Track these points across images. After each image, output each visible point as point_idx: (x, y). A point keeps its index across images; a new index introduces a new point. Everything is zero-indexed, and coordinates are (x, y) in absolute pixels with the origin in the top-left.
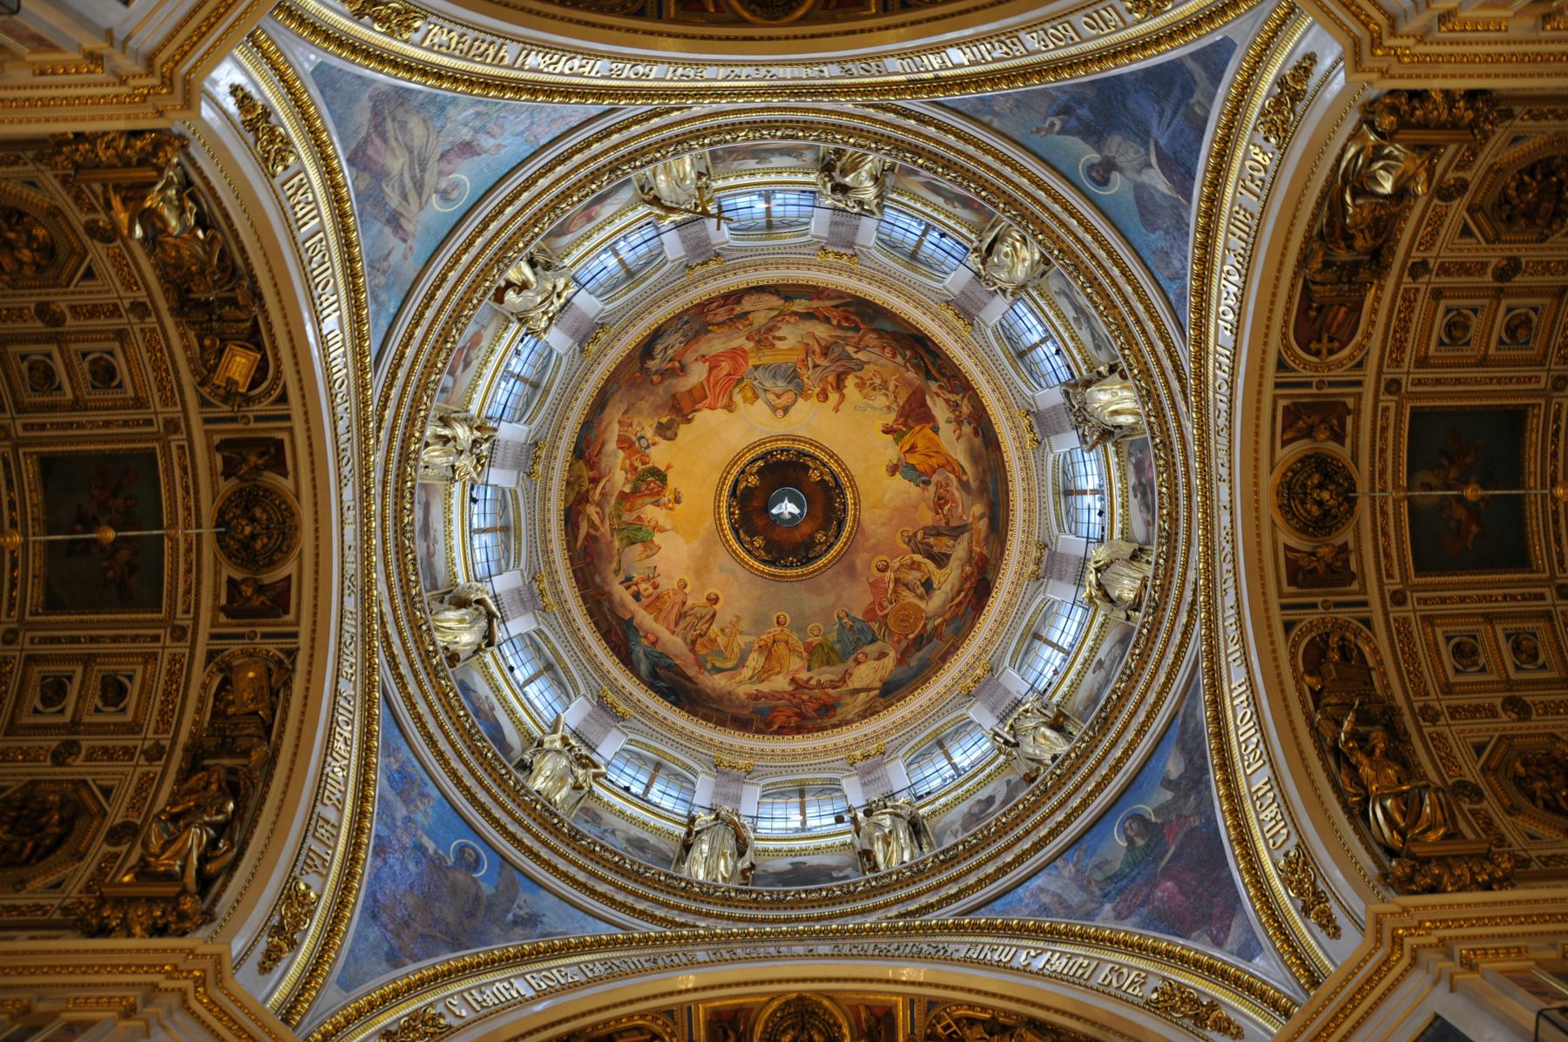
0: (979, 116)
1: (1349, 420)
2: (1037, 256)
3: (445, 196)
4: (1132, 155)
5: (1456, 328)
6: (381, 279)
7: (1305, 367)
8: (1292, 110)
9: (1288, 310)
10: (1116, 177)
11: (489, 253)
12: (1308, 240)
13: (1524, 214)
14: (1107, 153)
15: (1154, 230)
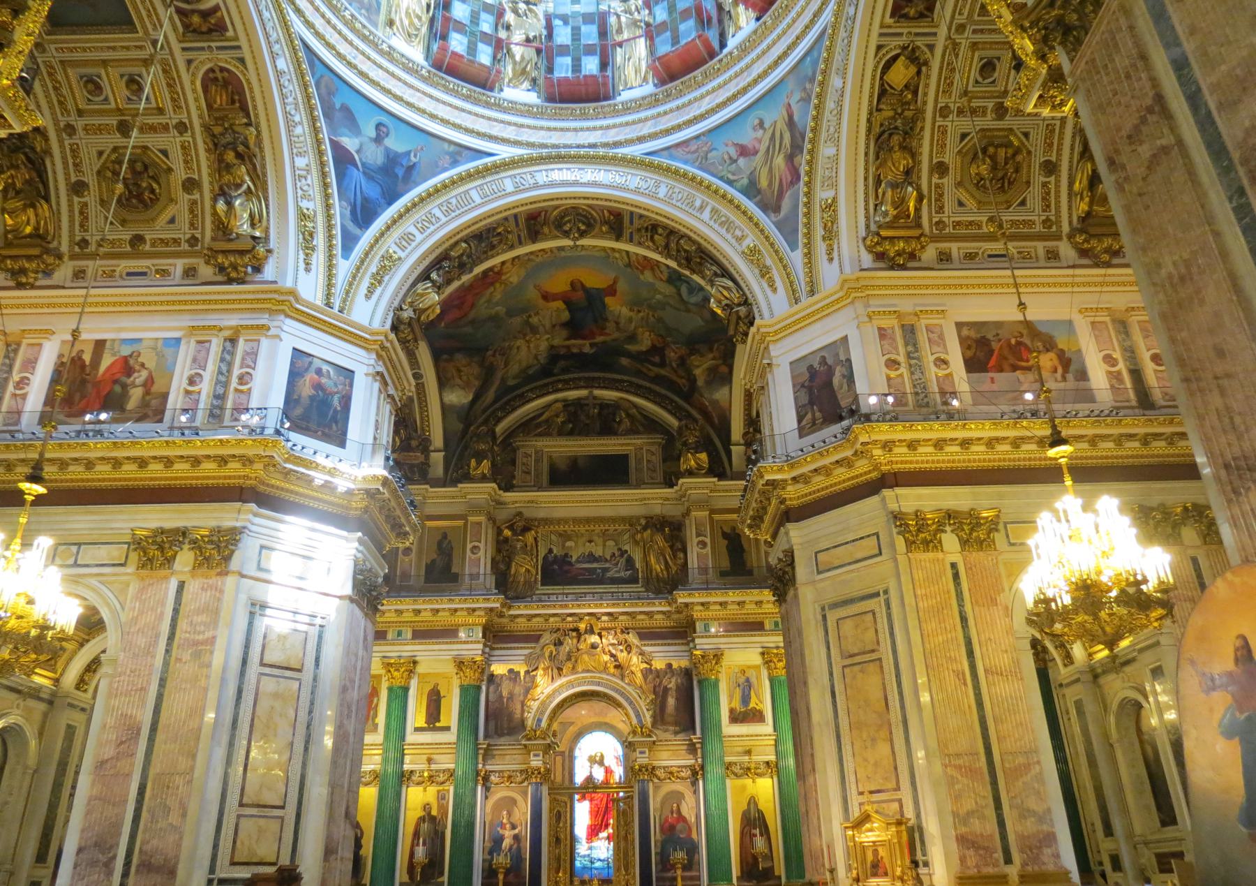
0: (458, 148)
1: (181, 30)
2: (398, 23)
3: (761, 124)
4: (368, 154)
5: (134, 84)
6: (808, 86)
7: (225, 59)
8: (303, 234)
9: (253, 99)
10: (373, 134)
11: (747, 60)
12: (261, 149)
13: (140, 173)
14: (381, 149)
15: (342, 105)
